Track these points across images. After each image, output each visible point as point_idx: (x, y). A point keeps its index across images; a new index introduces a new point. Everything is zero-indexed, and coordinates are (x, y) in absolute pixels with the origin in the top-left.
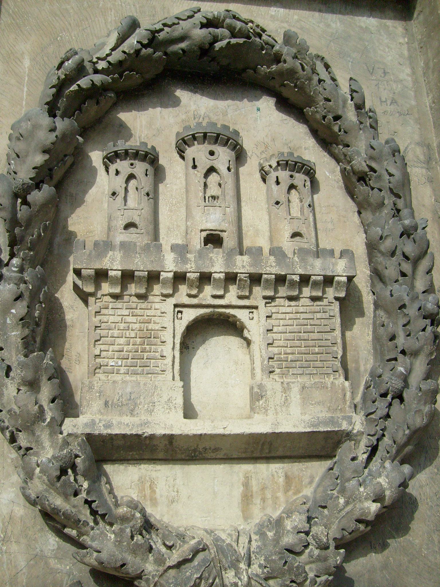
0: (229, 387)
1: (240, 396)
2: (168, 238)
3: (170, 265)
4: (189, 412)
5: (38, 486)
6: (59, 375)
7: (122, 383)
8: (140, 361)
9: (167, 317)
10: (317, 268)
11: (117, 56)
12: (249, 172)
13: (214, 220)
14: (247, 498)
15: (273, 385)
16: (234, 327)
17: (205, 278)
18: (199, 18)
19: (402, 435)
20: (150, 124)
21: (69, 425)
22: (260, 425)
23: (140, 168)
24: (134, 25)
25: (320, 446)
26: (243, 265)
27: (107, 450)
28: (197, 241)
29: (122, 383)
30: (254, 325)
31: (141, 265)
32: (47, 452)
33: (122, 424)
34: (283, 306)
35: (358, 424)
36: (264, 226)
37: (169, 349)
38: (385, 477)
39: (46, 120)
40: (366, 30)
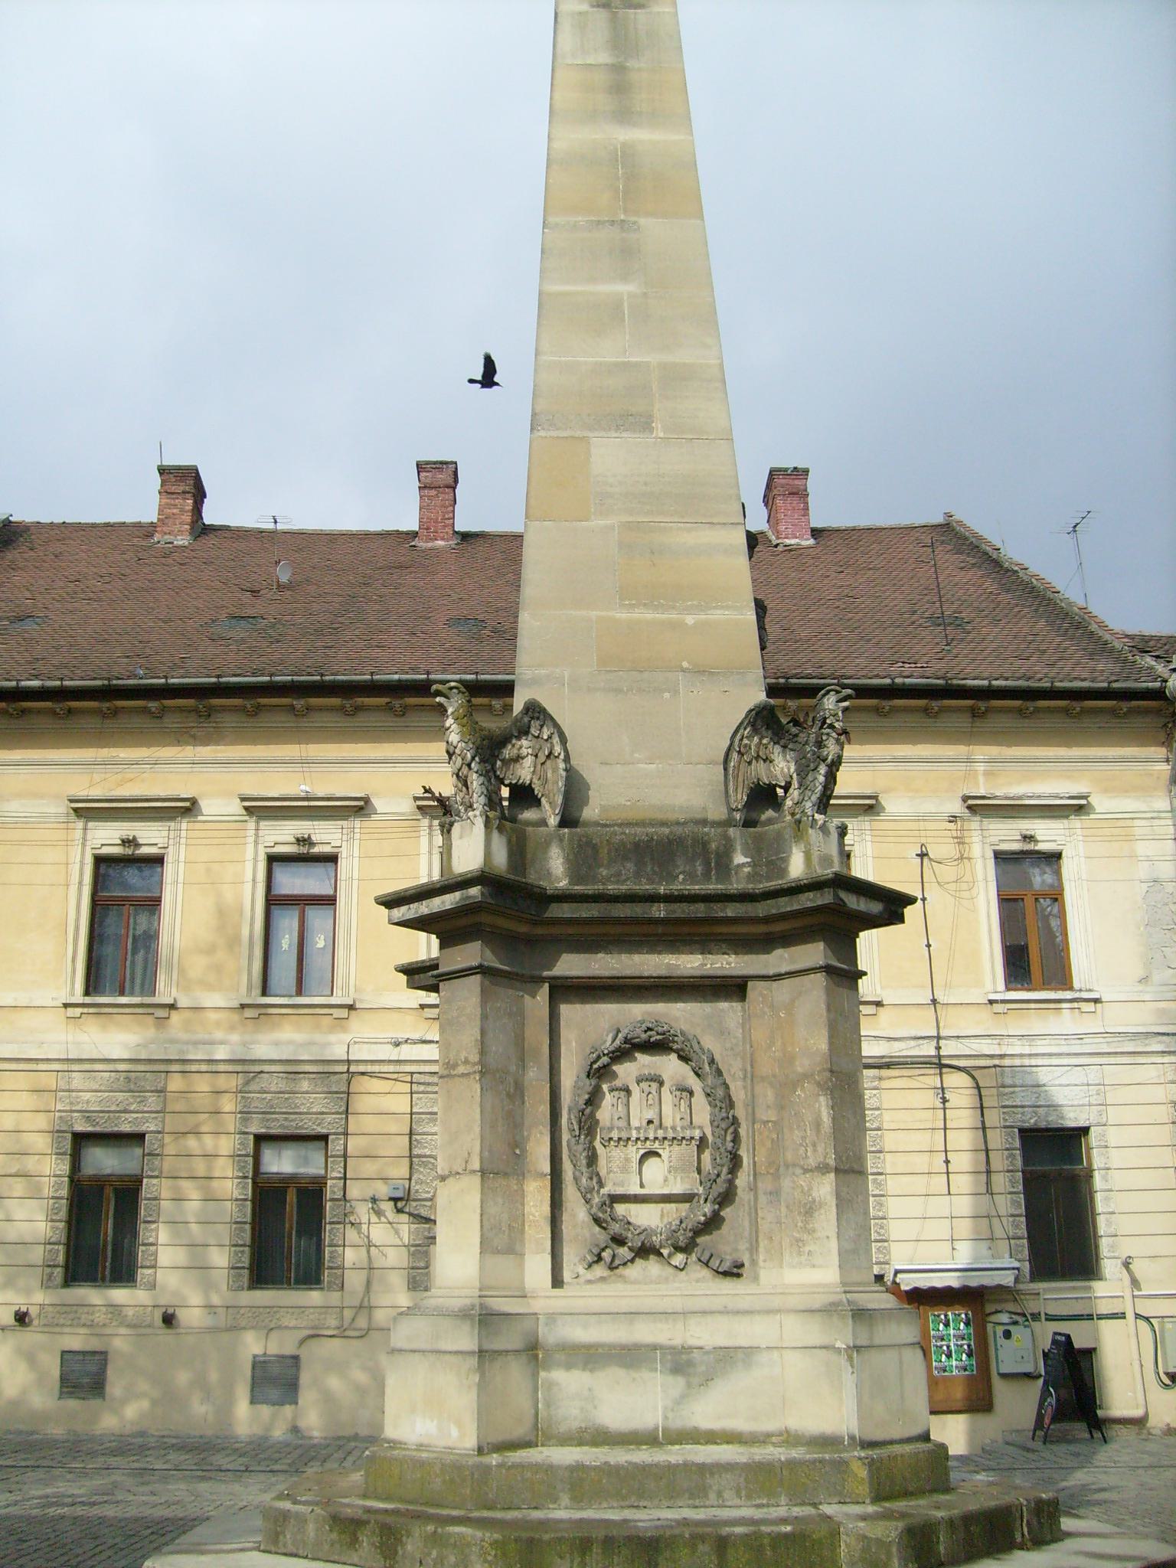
0: (657, 1176)
1: (661, 1180)
2: (635, 1123)
3: (634, 1134)
4: (642, 1186)
5: (594, 1210)
6: (598, 1174)
7: (620, 1177)
8: (624, 1169)
9: (634, 1152)
10: (688, 1134)
11: (611, 1049)
12: (665, 1090)
13: (651, 1114)
14: (662, 1216)
15: (671, 1177)
16: (658, 1155)
17: (647, 1139)
18: (644, 1027)
19: (716, 1194)
20: (626, 1071)
21: (602, 1191)
22: (666, 1191)
23: (623, 1094)
24: (618, 1031)
25: (687, 1198)
26: (660, 1134)
27: (615, 1199)
28: (644, 1123)
29: (620, 1177)
30: (665, 1154)
31: (624, 1135)
32: (596, 1200)
33: (620, 1191)
34: (676, 1148)
35: (701, 1190)
36: (670, 1113)
37: (635, 1165)
38: (708, 1209)
39: (588, 1081)
40: (722, 1010)
